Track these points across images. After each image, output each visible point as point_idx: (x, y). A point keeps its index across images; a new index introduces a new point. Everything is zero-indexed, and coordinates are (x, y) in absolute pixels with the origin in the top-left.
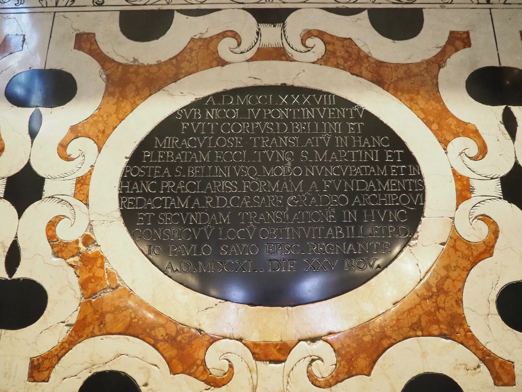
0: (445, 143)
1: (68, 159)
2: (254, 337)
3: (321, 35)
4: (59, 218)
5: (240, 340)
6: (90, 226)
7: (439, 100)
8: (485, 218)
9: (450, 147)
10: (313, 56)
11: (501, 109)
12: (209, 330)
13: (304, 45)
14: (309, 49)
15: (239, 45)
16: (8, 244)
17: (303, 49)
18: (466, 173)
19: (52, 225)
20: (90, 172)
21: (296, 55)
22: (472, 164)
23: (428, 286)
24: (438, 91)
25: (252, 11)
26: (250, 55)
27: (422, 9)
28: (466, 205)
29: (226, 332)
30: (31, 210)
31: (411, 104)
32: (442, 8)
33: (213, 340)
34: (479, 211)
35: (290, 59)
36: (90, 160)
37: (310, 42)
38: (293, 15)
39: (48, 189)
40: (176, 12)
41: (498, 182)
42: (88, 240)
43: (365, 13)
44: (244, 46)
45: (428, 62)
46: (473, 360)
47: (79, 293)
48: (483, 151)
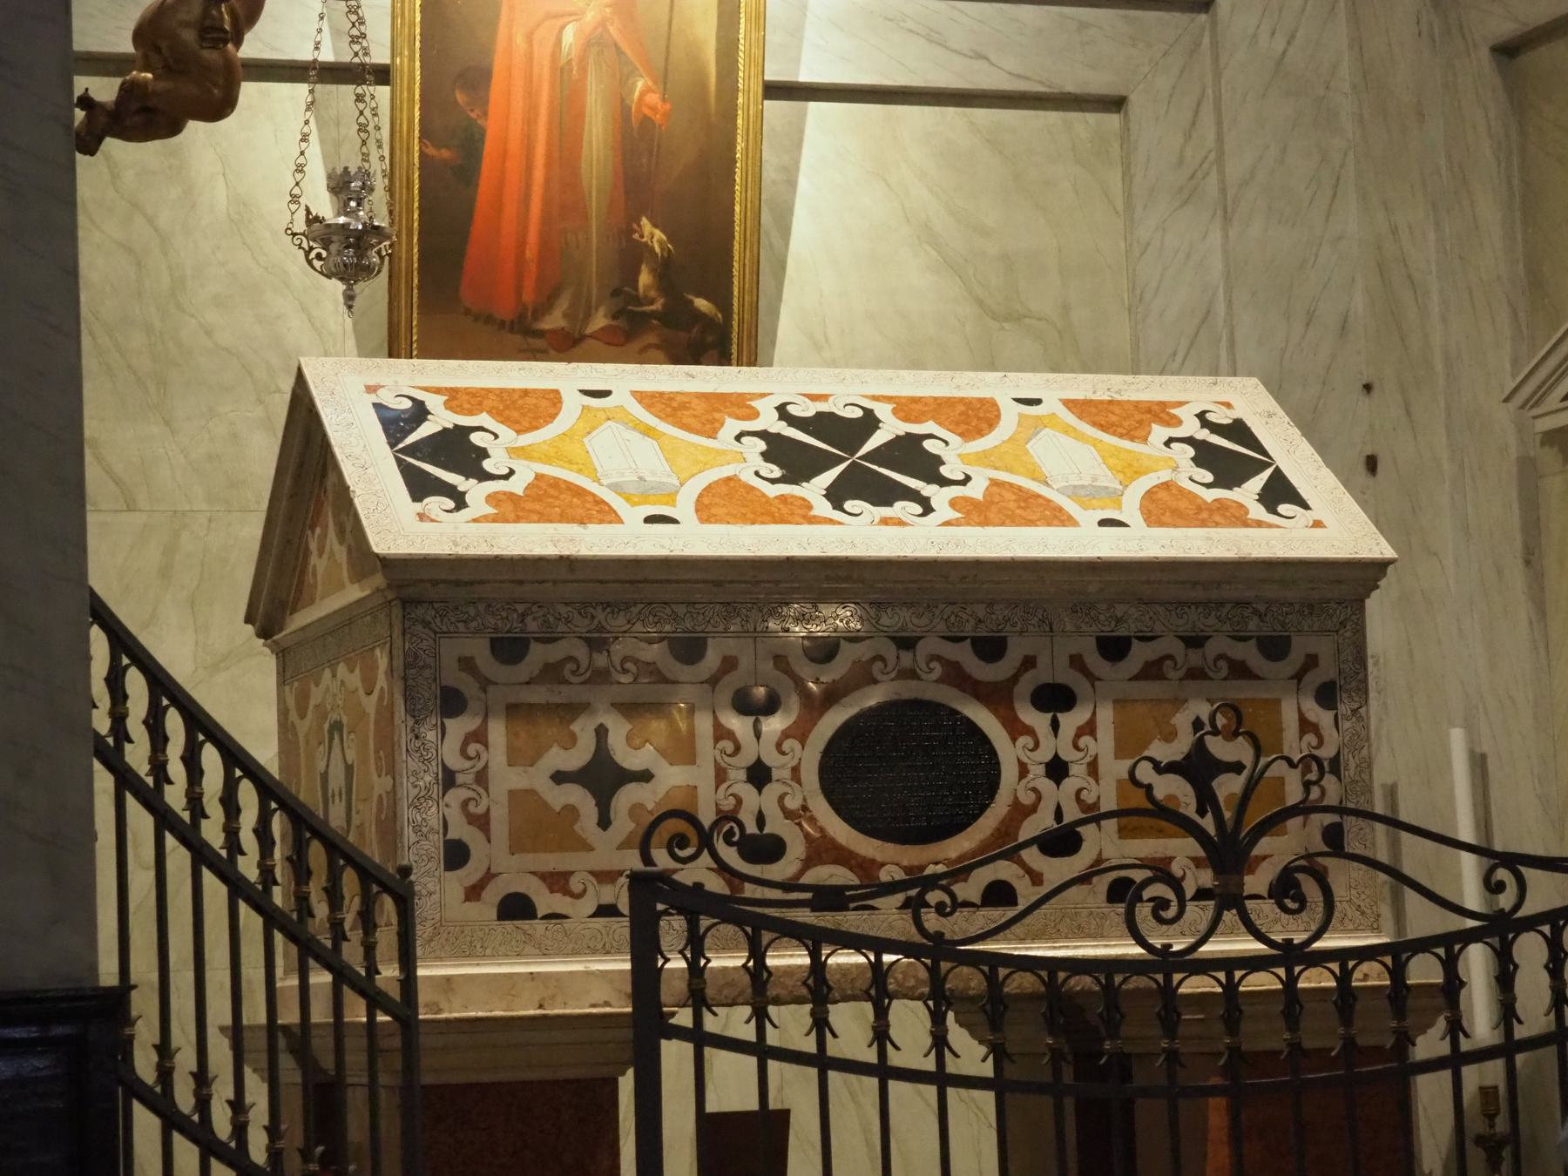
0: (1014, 740)
1: (783, 753)
2: (905, 863)
3: (938, 658)
4: (786, 794)
5: (897, 864)
6: (805, 800)
7: (1013, 709)
8: (1034, 790)
9: (1017, 743)
10: (935, 675)
11: (1049, 716)
12: (879, 858)
13: (928, 666)
14: (931, 671)
15: (886, 666)
16: (756, 812)
17: (927, 670)
18: (1025, 760)
19: (781, 798)
20: (799, 763)
21: (924, 676)
22: (1029, 753)
23: (998, 830)
24: (1012, 703)
25: (893, 639)
26: (893, 675)
27: (1006, 637)
28: (1024, 781)
29: (888, 860)
30: (766, 789)
31: (995, 712)
32: (1020, 635)
33: (883, 865)
34: (1030, 786)
35: (919, 679)
36: (798, 755)
37: (932, 665)
38: (922, 641)
39: (775, 774)
40: (842, 641)
41: (1043, 766)
42: (805, 808)
43: (969, 641)
44: (890, 667)
45: (1008, 680)
46: (1021, 872)
47: (804, 841)
48: (1037, 745)
